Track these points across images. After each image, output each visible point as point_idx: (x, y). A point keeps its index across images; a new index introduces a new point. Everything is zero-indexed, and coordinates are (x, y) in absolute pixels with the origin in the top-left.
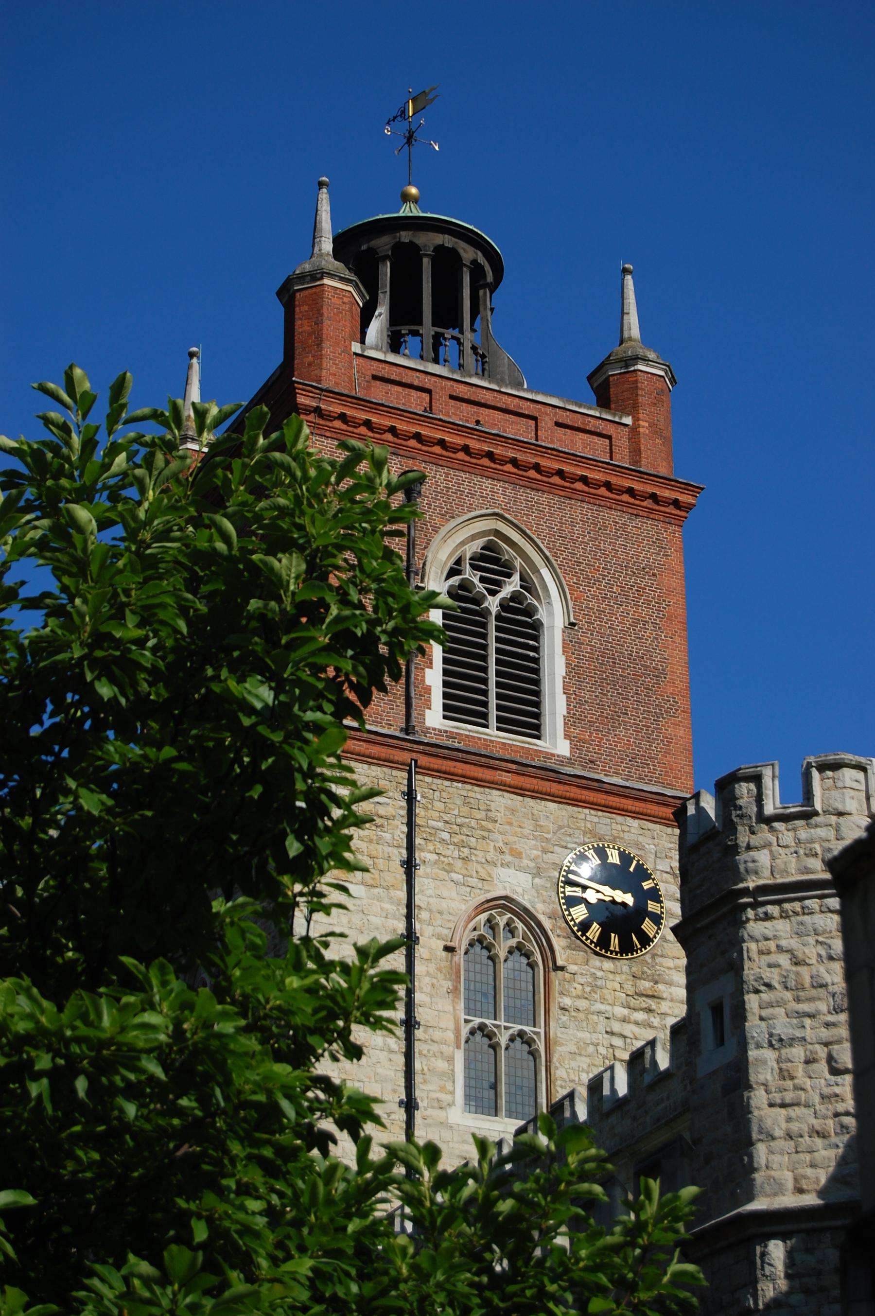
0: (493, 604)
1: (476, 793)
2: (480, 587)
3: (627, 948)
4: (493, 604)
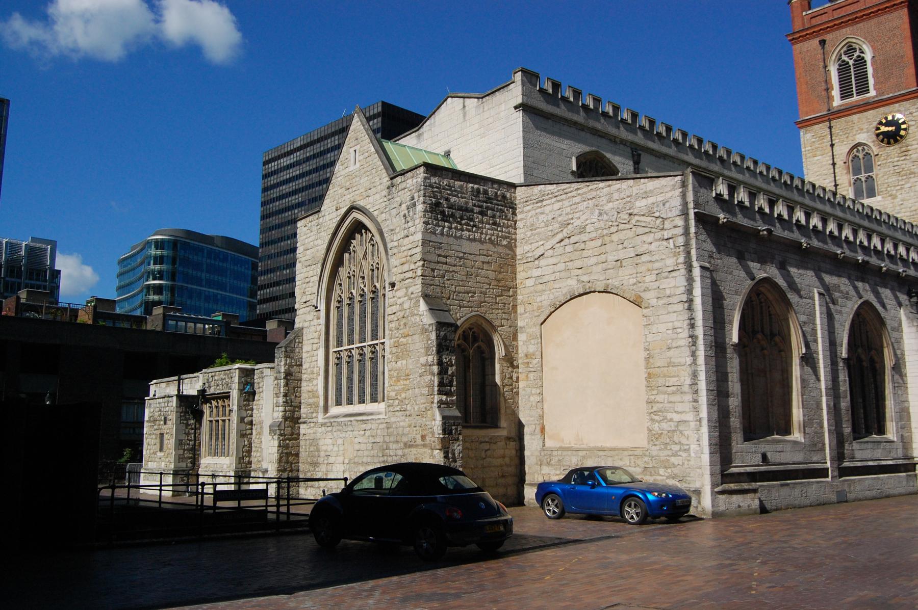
0: (851, 62)
1: (849, 118)
3: (896, 141)
4: (851, 62)
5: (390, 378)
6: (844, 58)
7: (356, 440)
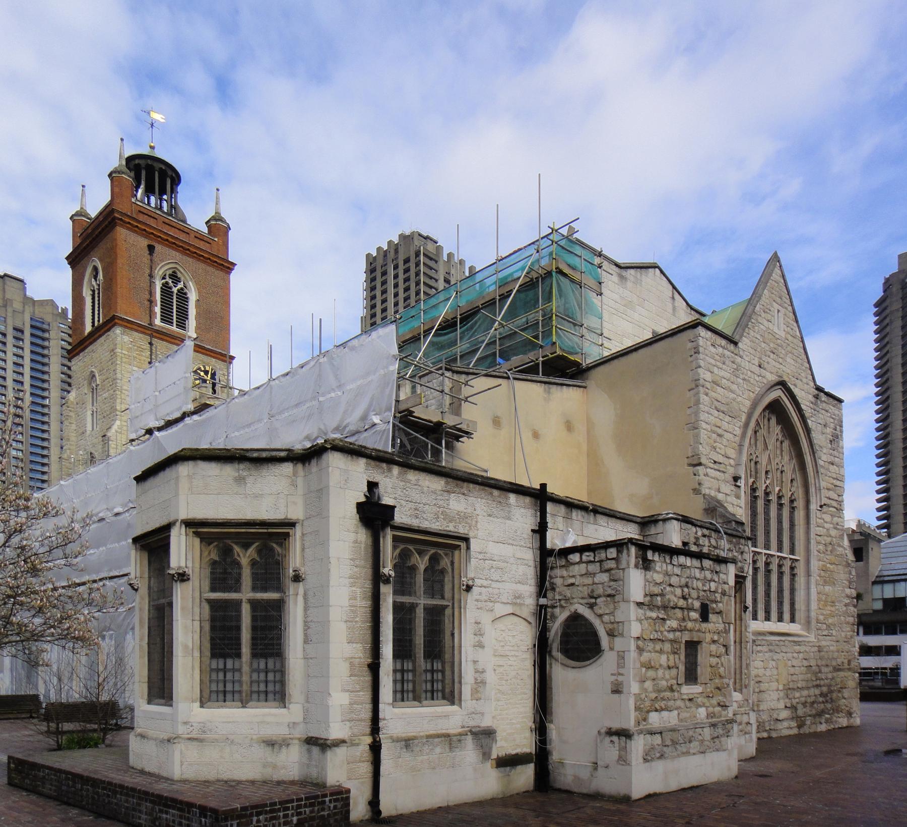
0: (175, 290)
2: (171, 284)
4: (175, 290)
5: (819, 600)
6: (170, 281)
7: (790, 663)
